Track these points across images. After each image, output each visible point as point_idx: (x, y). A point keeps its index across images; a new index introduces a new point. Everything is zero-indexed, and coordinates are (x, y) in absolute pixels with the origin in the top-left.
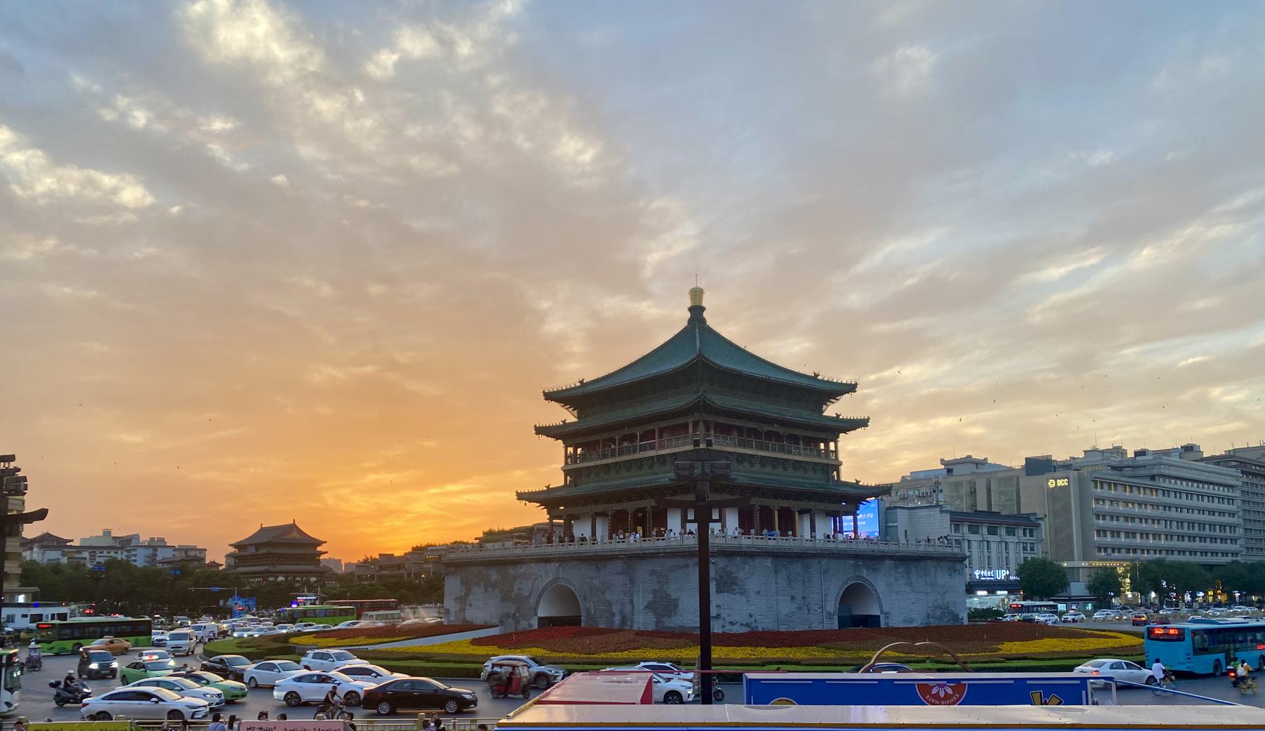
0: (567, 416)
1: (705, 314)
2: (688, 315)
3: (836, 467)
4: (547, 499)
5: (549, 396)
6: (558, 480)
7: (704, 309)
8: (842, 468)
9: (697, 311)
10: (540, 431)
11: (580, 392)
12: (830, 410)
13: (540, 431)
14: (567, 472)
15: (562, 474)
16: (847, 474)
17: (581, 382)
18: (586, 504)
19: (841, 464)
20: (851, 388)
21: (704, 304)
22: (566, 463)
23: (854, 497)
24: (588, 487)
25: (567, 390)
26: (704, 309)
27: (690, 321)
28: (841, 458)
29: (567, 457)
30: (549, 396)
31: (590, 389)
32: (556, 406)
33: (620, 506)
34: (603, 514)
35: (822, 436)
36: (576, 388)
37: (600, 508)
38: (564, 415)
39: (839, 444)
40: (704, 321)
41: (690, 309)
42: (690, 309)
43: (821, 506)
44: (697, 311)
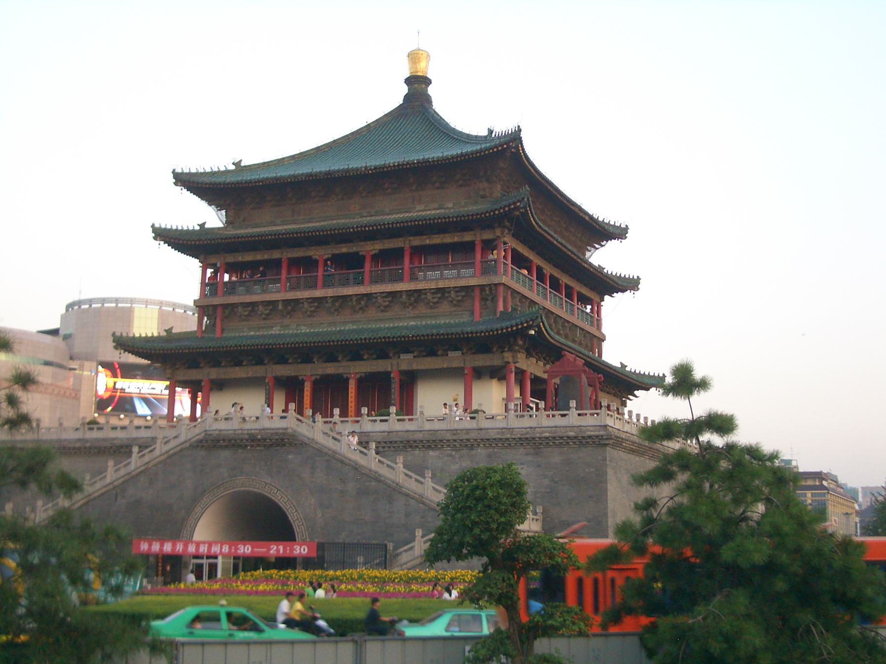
1: (431, 90)
2: (405, 89)
7: (427, 81)
8: (605, 345)
9: (418, 84)
10: (163, 235)
11: (234, 179)
13: (163, 235)
16: (612, 354)
17: (237, 164)
19: (602, 339)
21: (429, 76)
25: (213, 174)
26: (427, 81)
27: (407, 98)
28: (605, 329)
29: (203, 284)
31: (248, 177)
33: (331, 369)
36: (227, 172)
40: (428, 100)
41: (408, 81)
42: (408, 81)
44: (418, 84)
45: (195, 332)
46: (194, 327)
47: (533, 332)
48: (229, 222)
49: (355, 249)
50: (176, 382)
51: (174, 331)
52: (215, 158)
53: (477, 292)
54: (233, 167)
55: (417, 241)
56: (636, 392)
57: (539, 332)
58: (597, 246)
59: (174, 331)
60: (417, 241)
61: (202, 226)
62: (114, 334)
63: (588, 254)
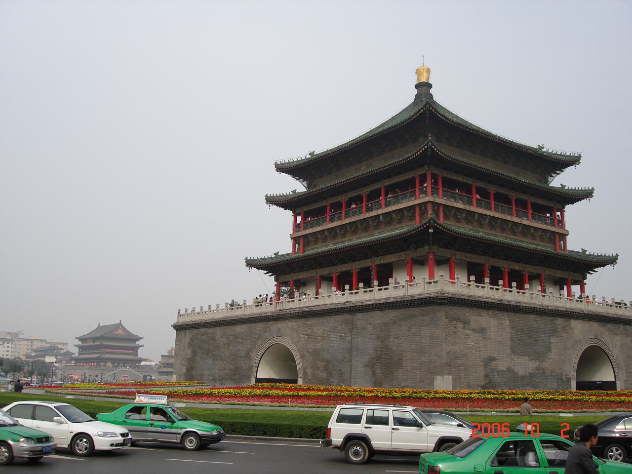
0: (295, 186)
1: (432, 91)
2: (415, 92)
3: (563, 236)
4: (275, 267)
5: (282, 168)
6: (285, 247)
7: (430, 86)
8: (568, 238)
10: (272, 201)
12: (557, 181)
13: (272, 201)
14: (295, 240)
15: (290, 242)
16: (574, 244)
18: (311, 268)
20: (574, 161)
21: (431, 82)
22: (295, 231)
23: (581, 267)
24: (312, 251)
26: (430, 86)
27: (417, 97)
29: (296, 225)
30: (282, 168)
32: (287, 177)
34: (328, 279)
35: (551, 204)
37: (325, 271)
38: (295, 186)
39: (565, 214)
40: (431, 96)
42: (418, 86)
43: (548, 272)
44: (424, 87)
45: (291, 254)
46: (290, 251)
47: (431, 231)
48: (308, 187)
49: (359, 193)
50: (280, 283)
51: (279, 254)
52: (299, 153)
53: (417, 209)
54: (310, 156)
55: (387, 183)
56: (596, 269)
57: (434, 228)
58: (558, 172)
59: (279, 254)
60: (387, 183)
61: (294, 192)
62: (246, 259)
63: (550, 179)
